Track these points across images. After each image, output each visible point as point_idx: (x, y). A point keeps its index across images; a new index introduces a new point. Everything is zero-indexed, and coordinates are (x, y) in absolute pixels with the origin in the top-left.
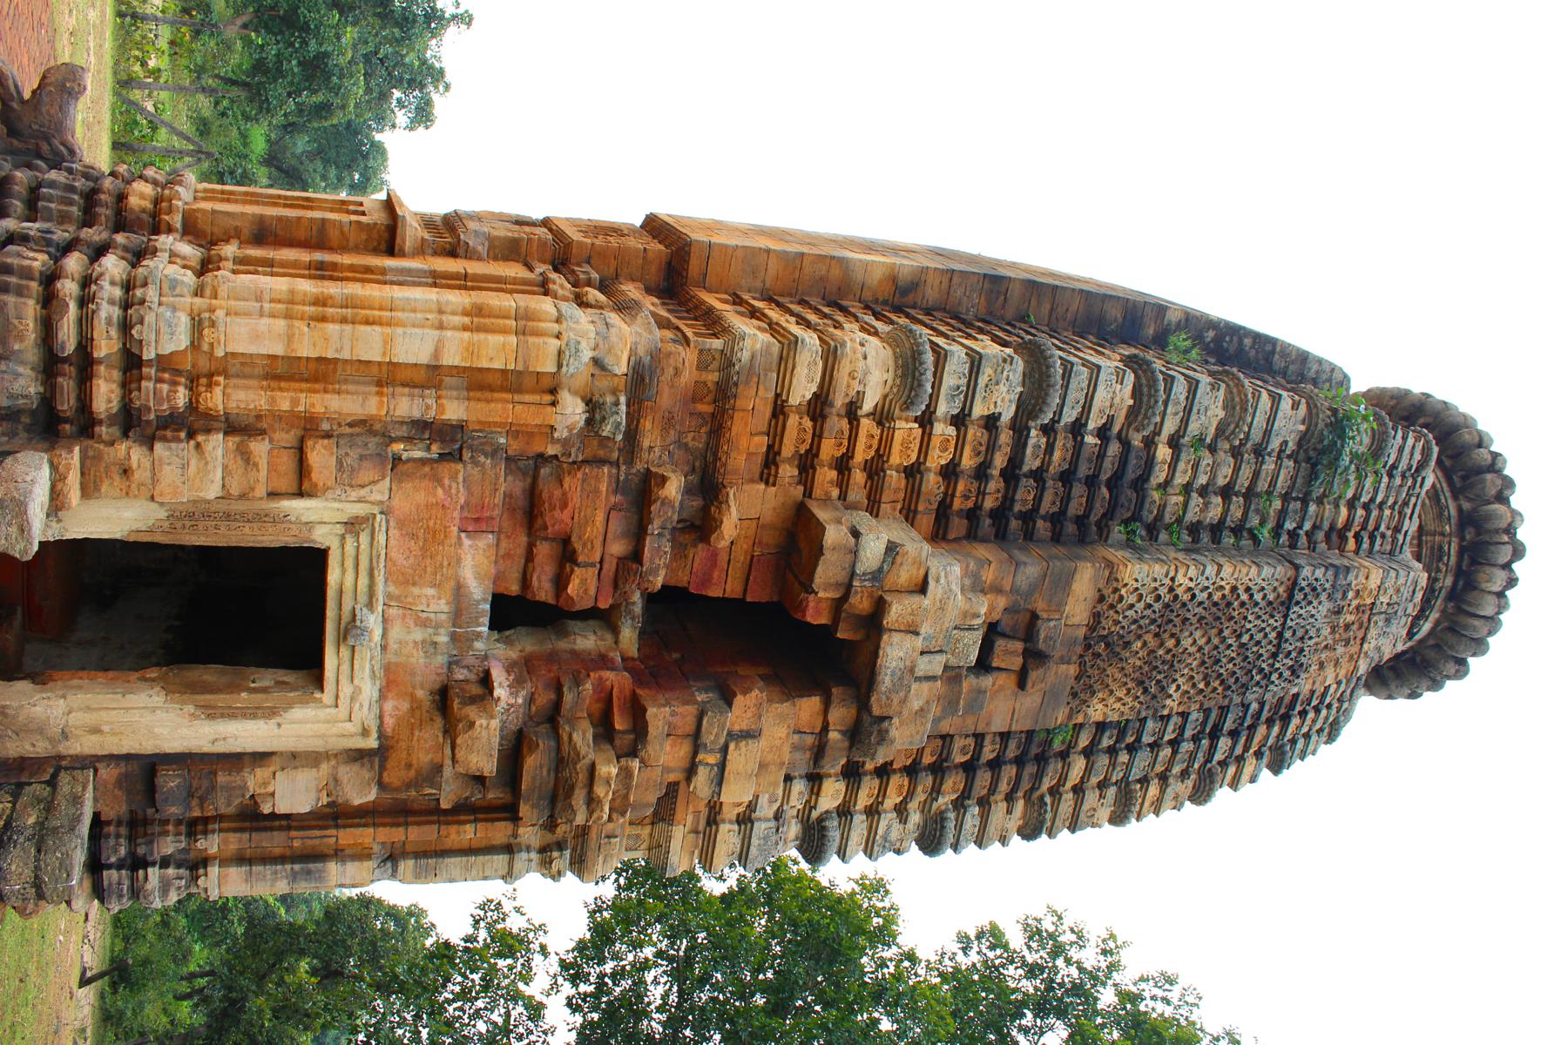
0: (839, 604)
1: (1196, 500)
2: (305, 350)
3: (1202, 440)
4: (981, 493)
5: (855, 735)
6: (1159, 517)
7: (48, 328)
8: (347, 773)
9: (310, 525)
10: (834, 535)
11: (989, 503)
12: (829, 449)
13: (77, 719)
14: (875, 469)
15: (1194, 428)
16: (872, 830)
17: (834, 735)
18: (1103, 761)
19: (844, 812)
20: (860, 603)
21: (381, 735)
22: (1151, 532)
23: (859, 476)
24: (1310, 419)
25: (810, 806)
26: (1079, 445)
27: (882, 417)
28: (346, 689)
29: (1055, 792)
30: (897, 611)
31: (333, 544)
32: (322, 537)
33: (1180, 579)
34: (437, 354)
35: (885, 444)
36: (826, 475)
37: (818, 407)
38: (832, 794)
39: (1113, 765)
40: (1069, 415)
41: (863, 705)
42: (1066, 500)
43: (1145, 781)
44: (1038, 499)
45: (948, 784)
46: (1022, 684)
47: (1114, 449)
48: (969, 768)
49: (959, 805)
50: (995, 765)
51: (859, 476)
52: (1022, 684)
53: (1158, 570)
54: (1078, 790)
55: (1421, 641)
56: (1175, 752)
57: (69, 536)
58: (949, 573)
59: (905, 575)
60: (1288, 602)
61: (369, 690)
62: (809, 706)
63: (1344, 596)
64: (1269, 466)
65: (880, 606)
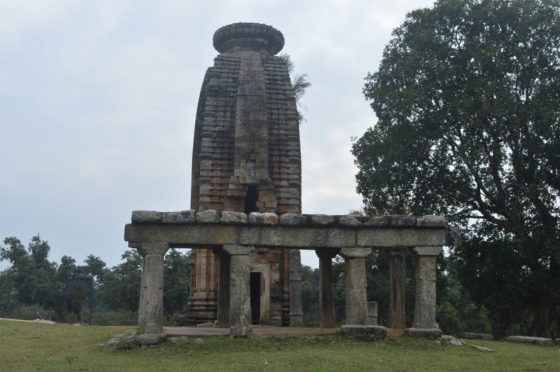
0: (241, 190)
1: (226, 119)
2: (205, 276)
3: (215, 121)
4: (225, 165)
6: (230, 127)
7: (203, 311)
8: (273, 268)
10: (229, 194)
12: (218, 194)
13: (264, 309)
14: (221, 185)
15: (212, 124)
16: (292, 174)
17: (266, 188)
18: (281, 126)
19: (288, 180)
20: (241, 187)
21: (268, 263)
22: (232, 127)
23: (223, 188)
24: (210, 96)
25: (286, 187)
26: (216, 147)
27: (213, 185)
28: (260, 269)
29: (287, 135)
30: (241, 182)
33: (238, 124)
34: (205, 257)
36: (223, 193)
37: (210, 196)
38: (284, 183)
39: (282, 124)
40: (211, 150)
41: (259, 185)
43: (286, 115)
44: (226, 153)
45: (283, 160)
46: (258, 153)
47: (217, 140)
48: (280, 156)
49: (287, 156)
51: (223, 188)
52: (258, 153)
53: (237, 129)
54: (287, 130)
55: (265, 39)
56: (281, 109)
58: (237, 172)
59: (236, 180)
60: (245, 96)
61: (260, 265)
62: (261, 193)
63: (244, 81)
64: (219, 103)
65: (241, 184)
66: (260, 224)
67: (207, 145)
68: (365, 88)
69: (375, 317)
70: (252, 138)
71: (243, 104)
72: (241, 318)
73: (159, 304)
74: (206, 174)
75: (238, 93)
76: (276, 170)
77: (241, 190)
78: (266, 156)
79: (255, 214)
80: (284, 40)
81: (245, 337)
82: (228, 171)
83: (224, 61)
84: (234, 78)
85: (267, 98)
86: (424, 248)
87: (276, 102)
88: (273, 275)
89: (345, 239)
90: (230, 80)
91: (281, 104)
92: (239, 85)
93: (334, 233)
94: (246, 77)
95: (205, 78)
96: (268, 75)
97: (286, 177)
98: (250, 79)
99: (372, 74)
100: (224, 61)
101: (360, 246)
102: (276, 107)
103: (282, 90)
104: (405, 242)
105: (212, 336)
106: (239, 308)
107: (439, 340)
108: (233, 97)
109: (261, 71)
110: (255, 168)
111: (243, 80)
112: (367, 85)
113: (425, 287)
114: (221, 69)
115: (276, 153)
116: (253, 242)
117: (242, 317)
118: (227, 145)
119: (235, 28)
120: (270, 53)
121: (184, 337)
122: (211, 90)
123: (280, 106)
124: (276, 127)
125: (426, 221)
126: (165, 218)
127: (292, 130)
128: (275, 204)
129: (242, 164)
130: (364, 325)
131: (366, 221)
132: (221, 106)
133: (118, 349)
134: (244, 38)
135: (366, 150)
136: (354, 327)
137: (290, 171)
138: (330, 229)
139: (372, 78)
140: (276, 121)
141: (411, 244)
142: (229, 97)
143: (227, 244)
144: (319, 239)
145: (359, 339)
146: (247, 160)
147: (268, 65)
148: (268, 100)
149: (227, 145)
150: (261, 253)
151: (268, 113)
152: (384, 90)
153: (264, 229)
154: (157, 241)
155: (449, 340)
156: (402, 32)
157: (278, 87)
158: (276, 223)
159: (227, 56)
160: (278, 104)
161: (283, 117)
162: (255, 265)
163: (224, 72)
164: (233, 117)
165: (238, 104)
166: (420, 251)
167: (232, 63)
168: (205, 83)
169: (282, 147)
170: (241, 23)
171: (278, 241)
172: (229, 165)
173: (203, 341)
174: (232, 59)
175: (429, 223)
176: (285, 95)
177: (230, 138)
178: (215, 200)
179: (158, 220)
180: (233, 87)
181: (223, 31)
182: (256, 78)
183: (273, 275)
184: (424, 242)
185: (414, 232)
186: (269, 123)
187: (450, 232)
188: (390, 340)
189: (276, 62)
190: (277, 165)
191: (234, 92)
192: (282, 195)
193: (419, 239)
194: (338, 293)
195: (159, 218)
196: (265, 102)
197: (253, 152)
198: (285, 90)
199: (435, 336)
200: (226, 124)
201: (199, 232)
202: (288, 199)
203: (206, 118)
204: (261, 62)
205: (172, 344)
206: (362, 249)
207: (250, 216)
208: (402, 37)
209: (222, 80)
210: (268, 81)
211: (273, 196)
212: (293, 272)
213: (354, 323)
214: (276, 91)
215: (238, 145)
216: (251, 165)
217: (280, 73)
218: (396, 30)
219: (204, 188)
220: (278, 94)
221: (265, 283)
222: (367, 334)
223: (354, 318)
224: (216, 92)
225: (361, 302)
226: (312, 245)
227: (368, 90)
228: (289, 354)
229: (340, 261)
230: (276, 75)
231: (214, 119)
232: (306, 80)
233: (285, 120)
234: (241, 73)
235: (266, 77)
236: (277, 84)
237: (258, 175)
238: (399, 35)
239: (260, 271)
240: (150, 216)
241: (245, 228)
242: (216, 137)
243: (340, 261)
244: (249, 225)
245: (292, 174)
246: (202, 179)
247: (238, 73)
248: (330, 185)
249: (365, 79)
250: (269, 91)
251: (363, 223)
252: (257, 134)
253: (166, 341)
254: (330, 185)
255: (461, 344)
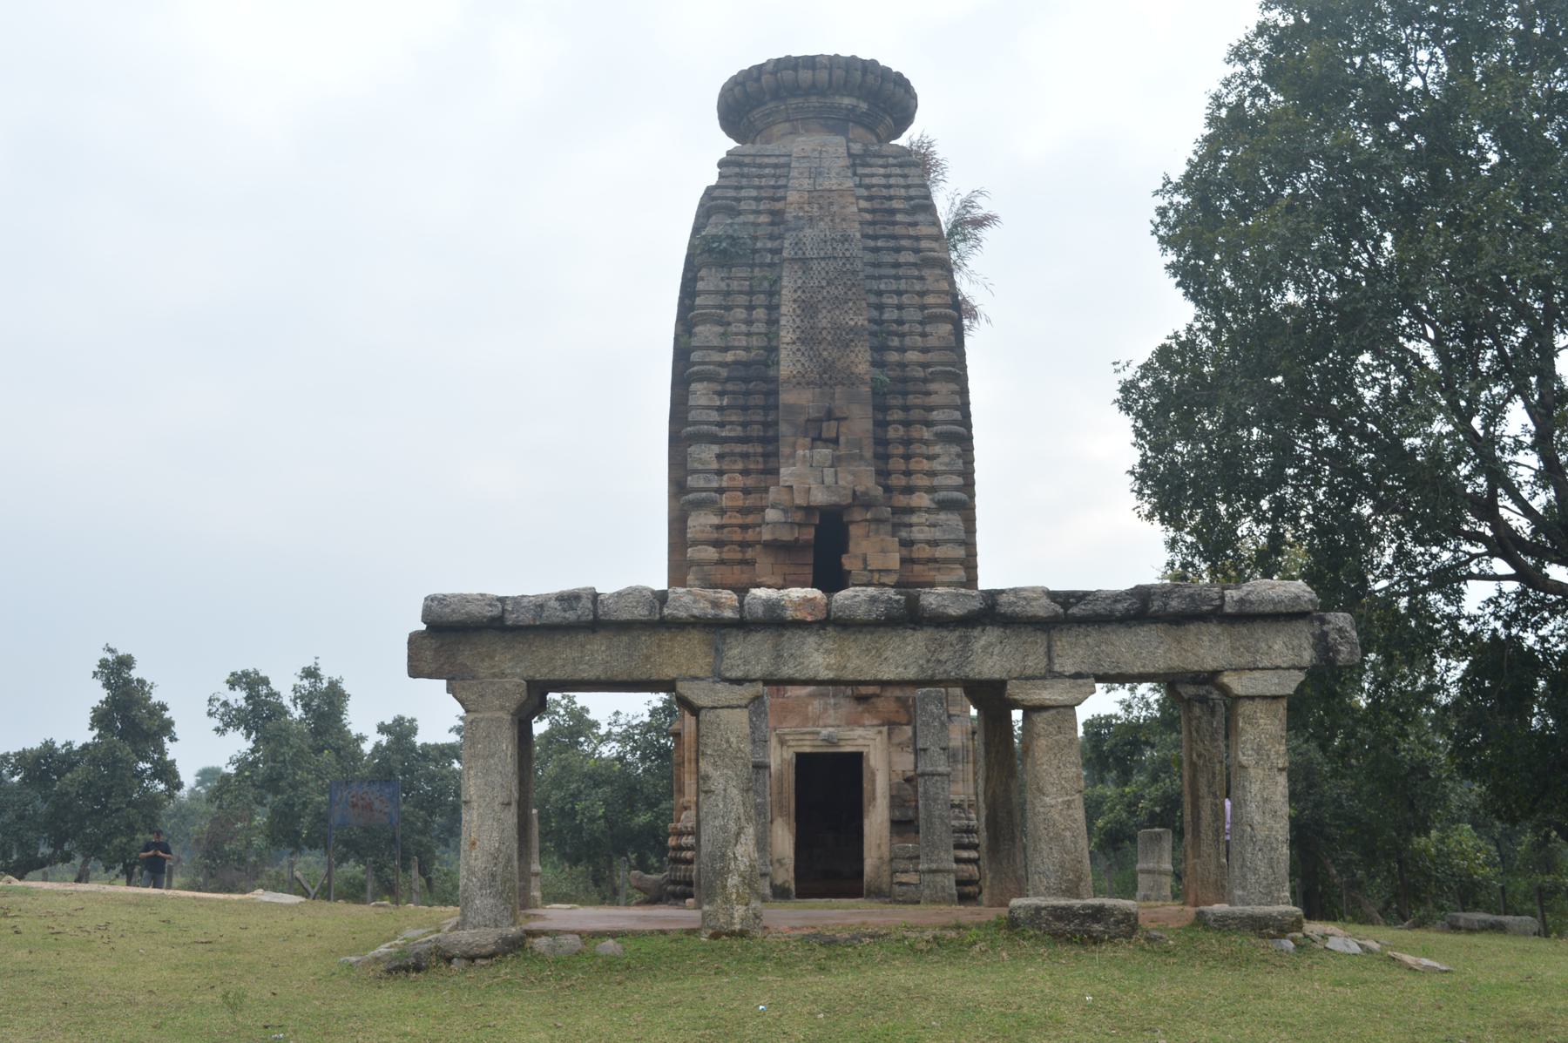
0: (799, 525)
1: (754, 329)
4: (755, 455)
5: (867, 506)
6: (765, 348)
8: (896, 740)
9: (783, 760)
10: (767, 535)
11: (759, 449)
12: (737, 537)
14: (744, 511)
15: (716, 342)
16: (944, 473)
17: (869, 516)
18: (908, 341)
19: (931, 490)
20: (799, 517)
21: (883, 725)
22: (773, 350)
23: (750, 519)
24: (708, 265)
25: (928, 510)
26: (729, 407)
27: (722, 512)
28: (860, 741)
29: (925, 366)
30: (799, 501)
31: (791, 751)
32: (789, 754)
33: (788, 340)
35: (733, 509)
36: (750, 535)
37: (717, 544)
39: (911, 333)
41: (849, 507)
42: (756, 407)
43: (923, 307)
45: (915, 435)
46: (845, 419)
47: (730, 387)
48: (907, 424)
49: (928, 424)
50: (906, 409)
51: (750, 519)
52: (845, 419)
53: (783, 354)
54: (925, 350)
55: (858, 98)
57: (792, 855)
58: (786, 473)
59: (784, 497)
60: (804, 261)
61: (859, 732)
62: (854, 531)
63: (801, 218)
64: (735, 285)
65: (799, 508)
66: (775, 622)
67: (703, 401)
68: (1158, 220)
69: (1165, 873)
70: (827, 377)
71: (800, 282)
72: (730, 882)
73: (503, 848)
74: (702, 484)
75: (785, 254)
76: (897, 464)
77: (799, 525)
78: (868, 425)
79: (761, 593)
80: (915, 97)
81: (742, 934)
82: (765, 472)
83: (746, 165)
84: (772, 213)
85: (866, 264)
86: (1248, 674)
87: (893, 272)
88: (896, 758)
89: (1018, 656)
90: (763, 219)
91: (907, 278)
92: (787, 230)
93: (985, 638)
94: (807, 208)
95: (697, 217)
96: (870, 198)
97: (923, 481)
98: (816, 212)
99: (1175, 179)
100: (746, 165)
101: (1061, 675)
102: (894, 287)
103: (910, 237)
104: (1193, 659)
105: (652, 932)
106: (724, 855)
107: (1293, 940)
108: (771, 265)
109: (849, 189)
110: (836, 462)
111: (797, 218)
112: (1162, 212)
113: (1255, 788)
114: (739, 188)
115: (897, 415)
116: (757, 671)
117: (733, 880)
118: (758, 400)
119: (774, 73)
120: (878, 136)
121: (569, 937)
122: (711, 251)
123: (903, 285)
124: (896, 342)
125: (1252, 597)
126: (512, 612)
127: (940, 349)
128: (894, 560)
129: (800, 452)
130: (1078, 896)
131: (1076, 604)
132: (741, 292)
133: (389, 971)
134: (801, 100)
135: (1168, 399)
136: (1044, 904)
137: (936, 465)
138: (974, 627)
139: (1177, 188)
140: (894, 327)
141: (1210, 664)
142: (761, 265)
143: (685, 679)
144: (943, 657)
145: (1057, 937)
146: (814, 440)
147: (867, 171)
148: (870, 270)
149: (758, 400)
150: (861, 699)
151: (869, 305)
152: (1208, 223)
153: (788, 634)
154: (494, 675)
155: (1325, 937)
156: (1254, 53)
157: (898, 230)
158: (821, 616)
159: (752, 151)
160: (897, 278)
161: (912, 314)
162: (845, 733)
163: (745, 199)
164: (773, 322)
165: (785, 282)
166: (1237, 684)
167: (767, 171)
168: (696, 230)
169: (912, 400)
170: (788, 57)
171: (828, 667)
172: (766, 456)
173: (619, 946)
174: (766, 160)
175: (1261, 602)
176: (917, 251)
177: (765, 380)
178: (731, 554)
179: (493, 619)
180: (772, 237)
181: (742, 84)
182: (835, 208)
183: (896, 758)
184: (1247, 659)
185: (1217, 630)
186: (873, 334)
187: (1325, 628)
188: (1149, 939)
189: (891, 160)
190: (901, 450)
191: (771, 251)
192: (917, 534)
193: (1234, 649)
194: (1130, 805)
195: (496, 612)
196: (861, 275)
197: (830, 415)
198: (917, 238)
199: (1282, 928)
200: (755, 342)
201: (608, 648)
202: (934, 543)
203: (698, 329)
204: (847, 162)
205: (538, 957)
206: (1068, 682)
207: (747, 599)
208: (1256, 67)
209: (741, 219)
210: (868, 217)
211: (889, 538)
212: (925, 750)
213: (1050, 892)
214: (892, 243)
215: (787, 397)
216: (824, 452)
217: (903, 192)
218: (1238, 48)
219: (700, 522)
220: (898, 250)
221: (873, 781)
222: (1082, 924)
223: (1048, 877)
224: (728, 253)
225: (1068, 833)
226: (922, 676)
227: (1166, 225)
228: (840, 982)
229: (1135, 713)
230: (890, 198)
231: (720, 329)
232: (984, 207)
233: (921, 323)
234: (792, 196)
235: (863, 204)
236: (894, 223)
237: (846, 480)
238: (1246, 62)
239: (860, 749)
240: (471, 608)
241: (735, 632)
242: (728, 380)
243: (1135, 713)
244: (744, 625)
245: (944, 473)
246: (691, 496)
247: (784, 198)
248: (1061, 498)
249: (1156, 193)
250: (871, 243)
251: (1066, 609)
252: (839, 365)
253: (521, 947)
254: (1061, 498)
255: (1358, 950)
